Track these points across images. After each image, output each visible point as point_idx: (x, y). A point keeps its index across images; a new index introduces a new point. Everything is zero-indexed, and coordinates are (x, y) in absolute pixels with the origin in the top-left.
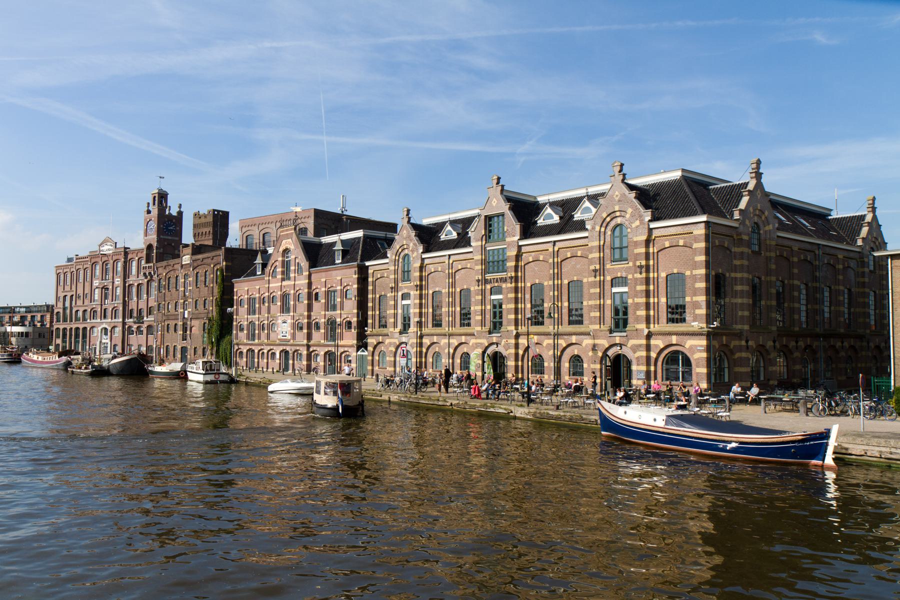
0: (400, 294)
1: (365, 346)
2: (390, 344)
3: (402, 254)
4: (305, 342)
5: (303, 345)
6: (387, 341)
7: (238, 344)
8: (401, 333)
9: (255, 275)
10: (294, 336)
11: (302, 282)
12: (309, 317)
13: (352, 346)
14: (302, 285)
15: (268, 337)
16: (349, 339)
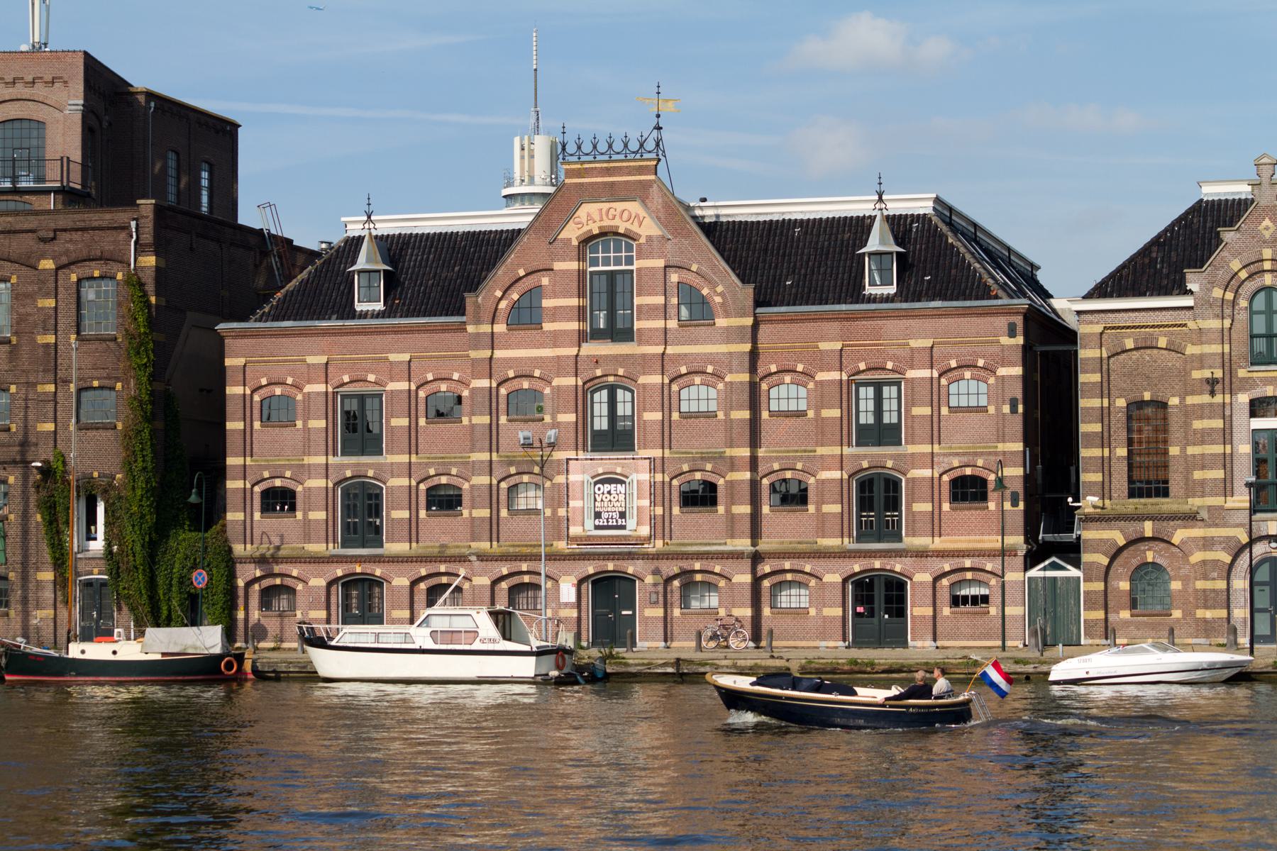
0: (1243, 398)
1: (1072, 552)
2: (1207, 544)
3: (1250, 287)
4: (743, 544)
5: (736, 555)
6: (1179, 536)
7: (261, 561)
8: (1253, 510)
9: (348, 312)
10: (661, 526)
11: (720, 344)
12: (754, 463)
13: (1004, 553)
14: (710, 359)
15: (493, 528)
16: (993, 530)
